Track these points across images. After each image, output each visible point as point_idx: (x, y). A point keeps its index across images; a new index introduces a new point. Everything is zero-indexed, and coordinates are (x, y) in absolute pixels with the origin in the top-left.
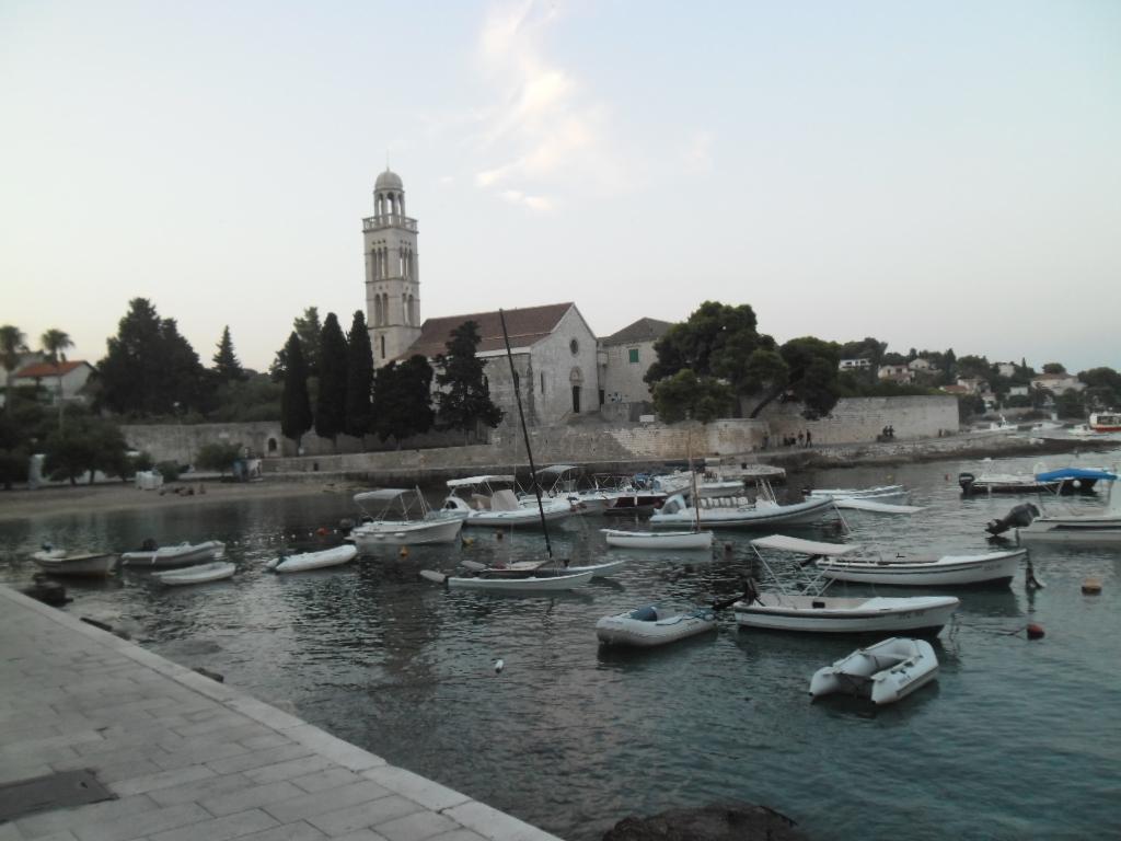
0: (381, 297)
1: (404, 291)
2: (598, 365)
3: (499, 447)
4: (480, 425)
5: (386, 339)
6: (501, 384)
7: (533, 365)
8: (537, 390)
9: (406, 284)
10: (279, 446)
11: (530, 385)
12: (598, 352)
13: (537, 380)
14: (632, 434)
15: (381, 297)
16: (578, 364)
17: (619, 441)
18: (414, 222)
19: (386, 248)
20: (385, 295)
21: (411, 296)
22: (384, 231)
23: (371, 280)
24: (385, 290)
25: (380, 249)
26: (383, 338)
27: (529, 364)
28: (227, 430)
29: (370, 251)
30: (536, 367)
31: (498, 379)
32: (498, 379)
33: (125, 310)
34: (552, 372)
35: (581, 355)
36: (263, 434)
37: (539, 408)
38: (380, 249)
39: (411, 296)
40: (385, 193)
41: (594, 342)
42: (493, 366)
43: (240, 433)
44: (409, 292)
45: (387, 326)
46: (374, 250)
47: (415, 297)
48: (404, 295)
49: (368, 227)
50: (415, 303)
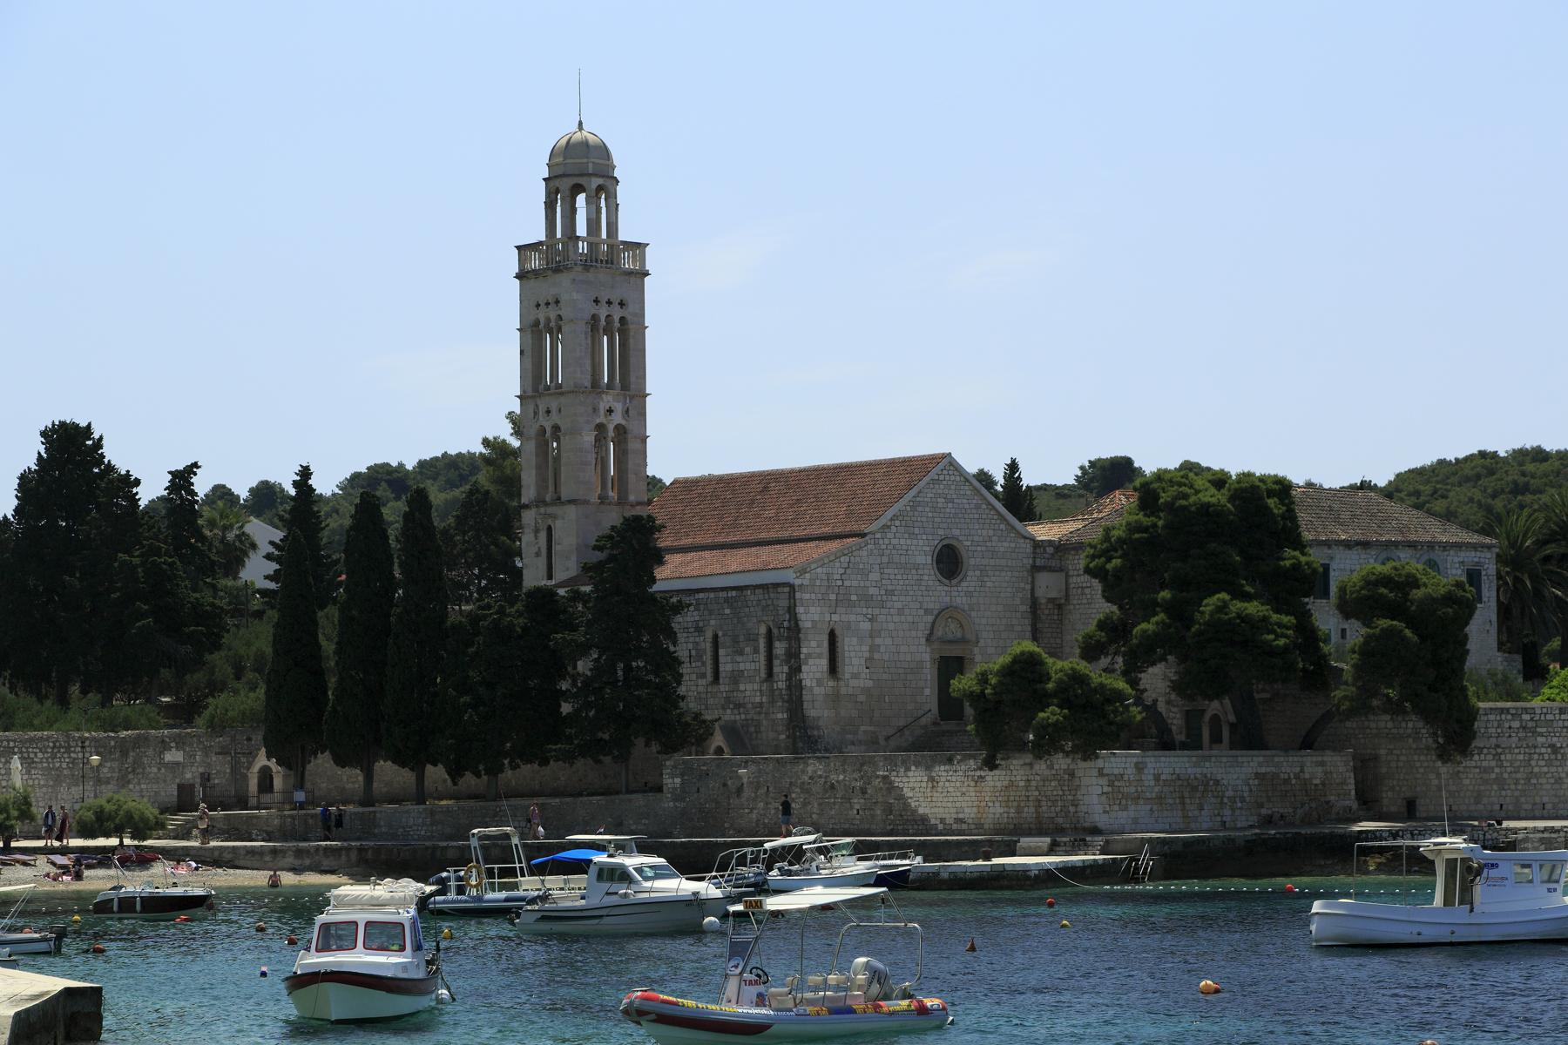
0: (548, 430)
1: (601, 419)
2: (1034, 604)
3: (675, 800)
4: (642, 750)
5: (556, 535)
6: (741, 653)
7: (800, 610)
8: (814, 670)
9: (607, 400)
10: (278, 783)
11: (794, 656)
12: (1035, 569)
13: (814, 650)
14: (932, 779)
15: (548, 430)
16: (961, 601)
17: (908, 793)
18: (638, 248)
19: (560, 317)
20: (556, 428)
21: (618, 428)
22: (559, 277)
23: (530, 393)
24: (555, 418)
25: (548, 320)
26: (549, 529)
27: (791, 610)
28: (180, 743)
29: (532, 318)
30: (811, 615)
31: (735, 641)
32: (735, 641)
33: (28, 452)
34: (866, 626)
35: (970, 581)
36: (252, 755)
37: (817, 709)
38: (548, 320)
39: (621, 431)
40: (566, 184)
41: (1029, 549)
42: (727, 611)
43: (206, 751)
44: (617, 418)
45: (558, 500)
46: (537, 323)
47: (632, 426)
48: (601, 428)
49: (535, 263)
50: (633, 445)
